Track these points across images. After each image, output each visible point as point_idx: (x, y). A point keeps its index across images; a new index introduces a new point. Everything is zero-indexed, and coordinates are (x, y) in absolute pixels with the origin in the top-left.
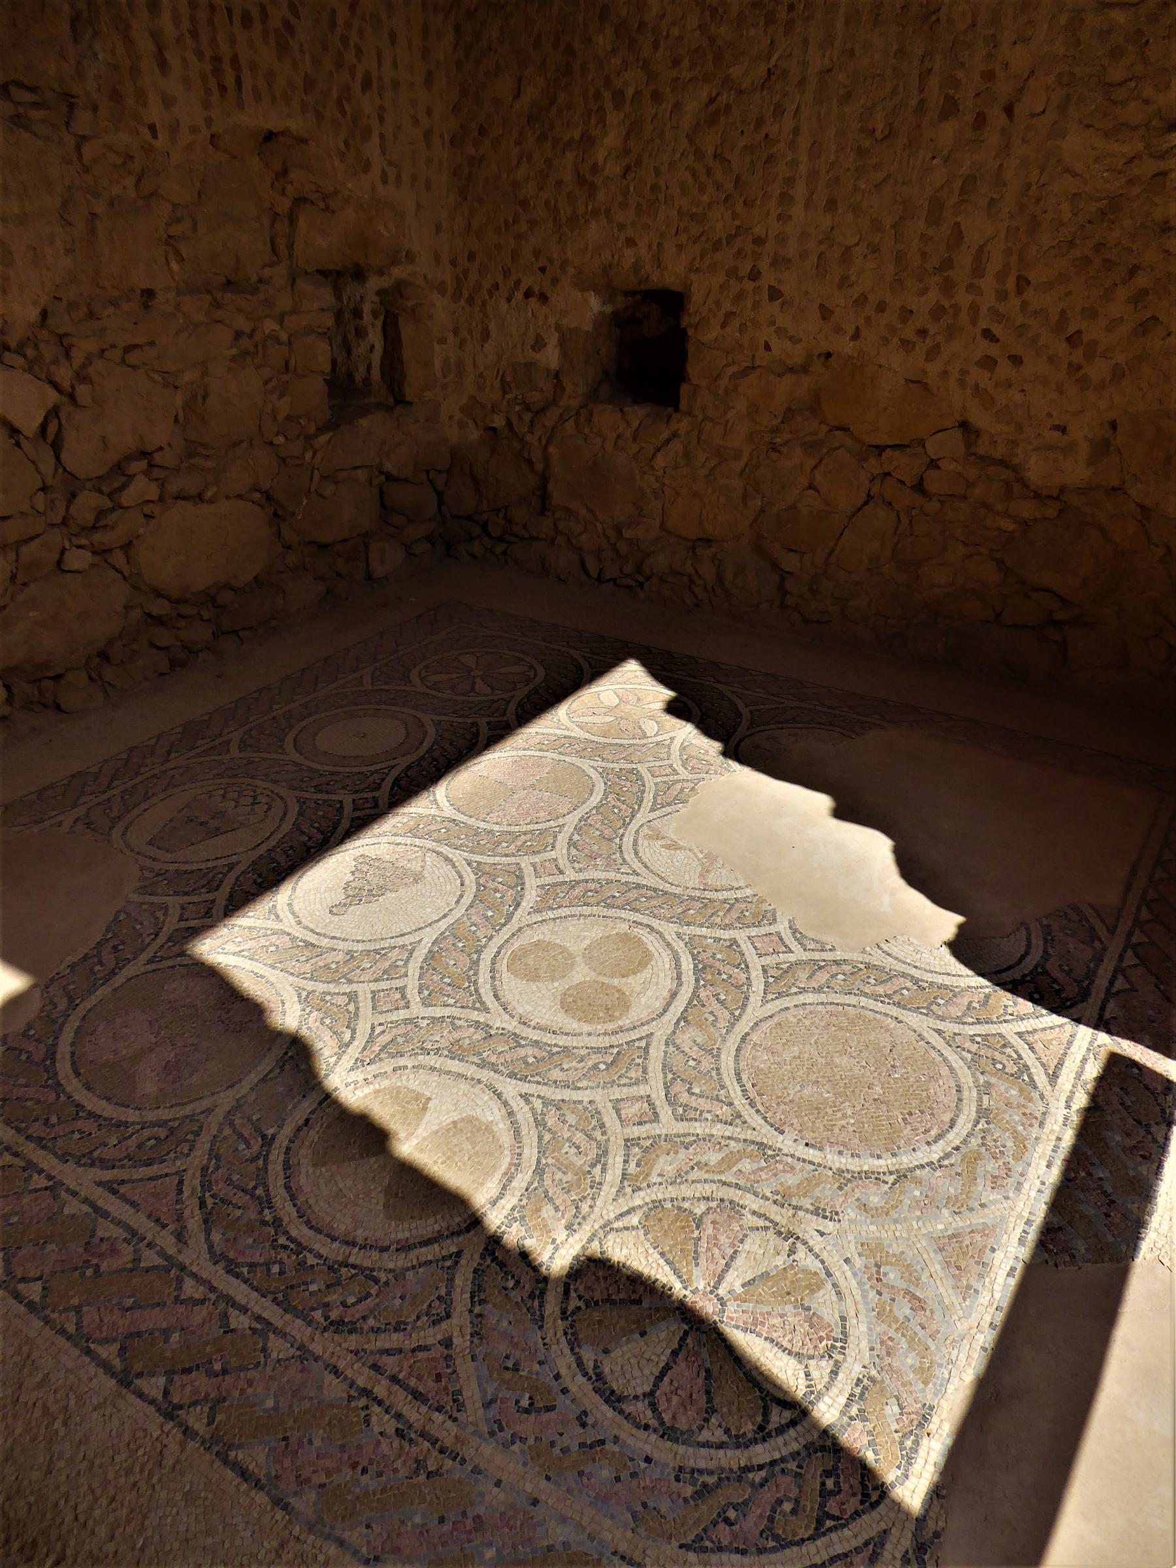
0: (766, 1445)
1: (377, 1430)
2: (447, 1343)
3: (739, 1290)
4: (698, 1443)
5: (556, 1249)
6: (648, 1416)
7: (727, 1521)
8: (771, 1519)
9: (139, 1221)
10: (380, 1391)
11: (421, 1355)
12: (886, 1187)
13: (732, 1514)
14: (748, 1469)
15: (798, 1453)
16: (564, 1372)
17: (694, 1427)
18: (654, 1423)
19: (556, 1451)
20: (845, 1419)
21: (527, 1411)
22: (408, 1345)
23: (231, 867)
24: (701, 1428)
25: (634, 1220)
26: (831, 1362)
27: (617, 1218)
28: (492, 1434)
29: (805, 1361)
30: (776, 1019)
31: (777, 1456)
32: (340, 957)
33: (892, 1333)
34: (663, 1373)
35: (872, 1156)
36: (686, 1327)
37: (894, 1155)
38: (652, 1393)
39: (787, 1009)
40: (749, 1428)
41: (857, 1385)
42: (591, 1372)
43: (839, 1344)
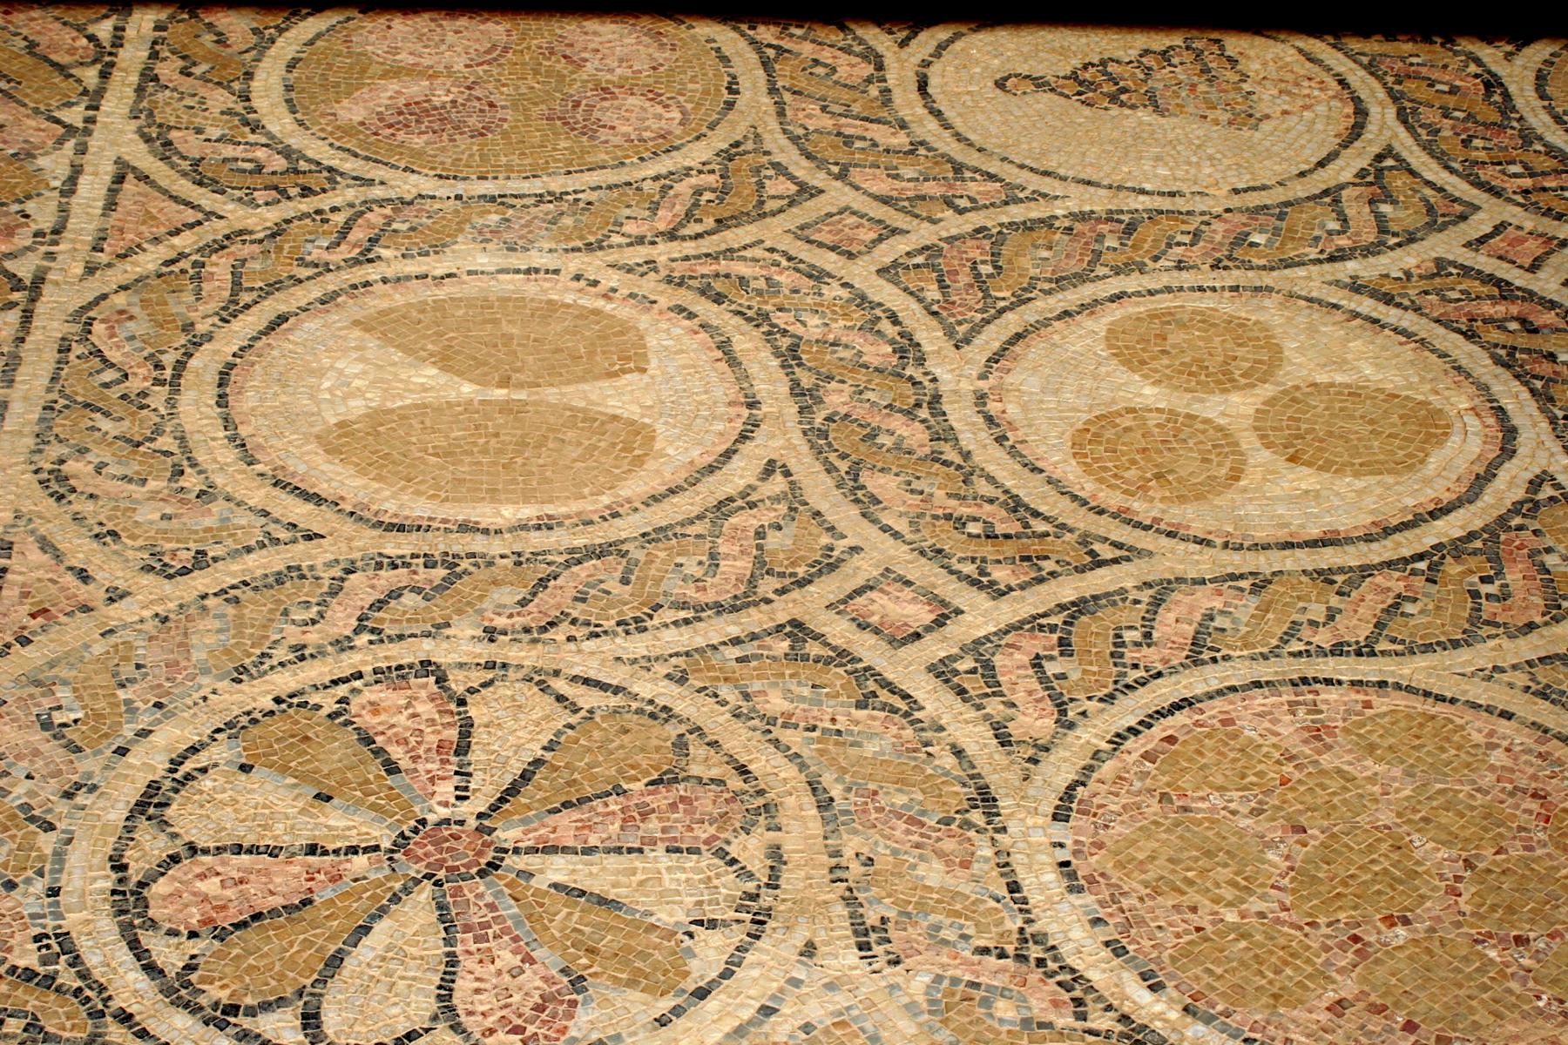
0: (200, 1027)
2: (115, 596)
4: (137, 941)
5: (428, 634)
11: (70, 580)
12: (1065, 1020)
18: (134, 874)
21: (46, 725)
25: (588, 698)
27: (574, 679)
29: (441, 1026)
30: (1440, 708)
32: (901, 140)
38: (193, 849)
40: (218, 993)
42: (188, 766)
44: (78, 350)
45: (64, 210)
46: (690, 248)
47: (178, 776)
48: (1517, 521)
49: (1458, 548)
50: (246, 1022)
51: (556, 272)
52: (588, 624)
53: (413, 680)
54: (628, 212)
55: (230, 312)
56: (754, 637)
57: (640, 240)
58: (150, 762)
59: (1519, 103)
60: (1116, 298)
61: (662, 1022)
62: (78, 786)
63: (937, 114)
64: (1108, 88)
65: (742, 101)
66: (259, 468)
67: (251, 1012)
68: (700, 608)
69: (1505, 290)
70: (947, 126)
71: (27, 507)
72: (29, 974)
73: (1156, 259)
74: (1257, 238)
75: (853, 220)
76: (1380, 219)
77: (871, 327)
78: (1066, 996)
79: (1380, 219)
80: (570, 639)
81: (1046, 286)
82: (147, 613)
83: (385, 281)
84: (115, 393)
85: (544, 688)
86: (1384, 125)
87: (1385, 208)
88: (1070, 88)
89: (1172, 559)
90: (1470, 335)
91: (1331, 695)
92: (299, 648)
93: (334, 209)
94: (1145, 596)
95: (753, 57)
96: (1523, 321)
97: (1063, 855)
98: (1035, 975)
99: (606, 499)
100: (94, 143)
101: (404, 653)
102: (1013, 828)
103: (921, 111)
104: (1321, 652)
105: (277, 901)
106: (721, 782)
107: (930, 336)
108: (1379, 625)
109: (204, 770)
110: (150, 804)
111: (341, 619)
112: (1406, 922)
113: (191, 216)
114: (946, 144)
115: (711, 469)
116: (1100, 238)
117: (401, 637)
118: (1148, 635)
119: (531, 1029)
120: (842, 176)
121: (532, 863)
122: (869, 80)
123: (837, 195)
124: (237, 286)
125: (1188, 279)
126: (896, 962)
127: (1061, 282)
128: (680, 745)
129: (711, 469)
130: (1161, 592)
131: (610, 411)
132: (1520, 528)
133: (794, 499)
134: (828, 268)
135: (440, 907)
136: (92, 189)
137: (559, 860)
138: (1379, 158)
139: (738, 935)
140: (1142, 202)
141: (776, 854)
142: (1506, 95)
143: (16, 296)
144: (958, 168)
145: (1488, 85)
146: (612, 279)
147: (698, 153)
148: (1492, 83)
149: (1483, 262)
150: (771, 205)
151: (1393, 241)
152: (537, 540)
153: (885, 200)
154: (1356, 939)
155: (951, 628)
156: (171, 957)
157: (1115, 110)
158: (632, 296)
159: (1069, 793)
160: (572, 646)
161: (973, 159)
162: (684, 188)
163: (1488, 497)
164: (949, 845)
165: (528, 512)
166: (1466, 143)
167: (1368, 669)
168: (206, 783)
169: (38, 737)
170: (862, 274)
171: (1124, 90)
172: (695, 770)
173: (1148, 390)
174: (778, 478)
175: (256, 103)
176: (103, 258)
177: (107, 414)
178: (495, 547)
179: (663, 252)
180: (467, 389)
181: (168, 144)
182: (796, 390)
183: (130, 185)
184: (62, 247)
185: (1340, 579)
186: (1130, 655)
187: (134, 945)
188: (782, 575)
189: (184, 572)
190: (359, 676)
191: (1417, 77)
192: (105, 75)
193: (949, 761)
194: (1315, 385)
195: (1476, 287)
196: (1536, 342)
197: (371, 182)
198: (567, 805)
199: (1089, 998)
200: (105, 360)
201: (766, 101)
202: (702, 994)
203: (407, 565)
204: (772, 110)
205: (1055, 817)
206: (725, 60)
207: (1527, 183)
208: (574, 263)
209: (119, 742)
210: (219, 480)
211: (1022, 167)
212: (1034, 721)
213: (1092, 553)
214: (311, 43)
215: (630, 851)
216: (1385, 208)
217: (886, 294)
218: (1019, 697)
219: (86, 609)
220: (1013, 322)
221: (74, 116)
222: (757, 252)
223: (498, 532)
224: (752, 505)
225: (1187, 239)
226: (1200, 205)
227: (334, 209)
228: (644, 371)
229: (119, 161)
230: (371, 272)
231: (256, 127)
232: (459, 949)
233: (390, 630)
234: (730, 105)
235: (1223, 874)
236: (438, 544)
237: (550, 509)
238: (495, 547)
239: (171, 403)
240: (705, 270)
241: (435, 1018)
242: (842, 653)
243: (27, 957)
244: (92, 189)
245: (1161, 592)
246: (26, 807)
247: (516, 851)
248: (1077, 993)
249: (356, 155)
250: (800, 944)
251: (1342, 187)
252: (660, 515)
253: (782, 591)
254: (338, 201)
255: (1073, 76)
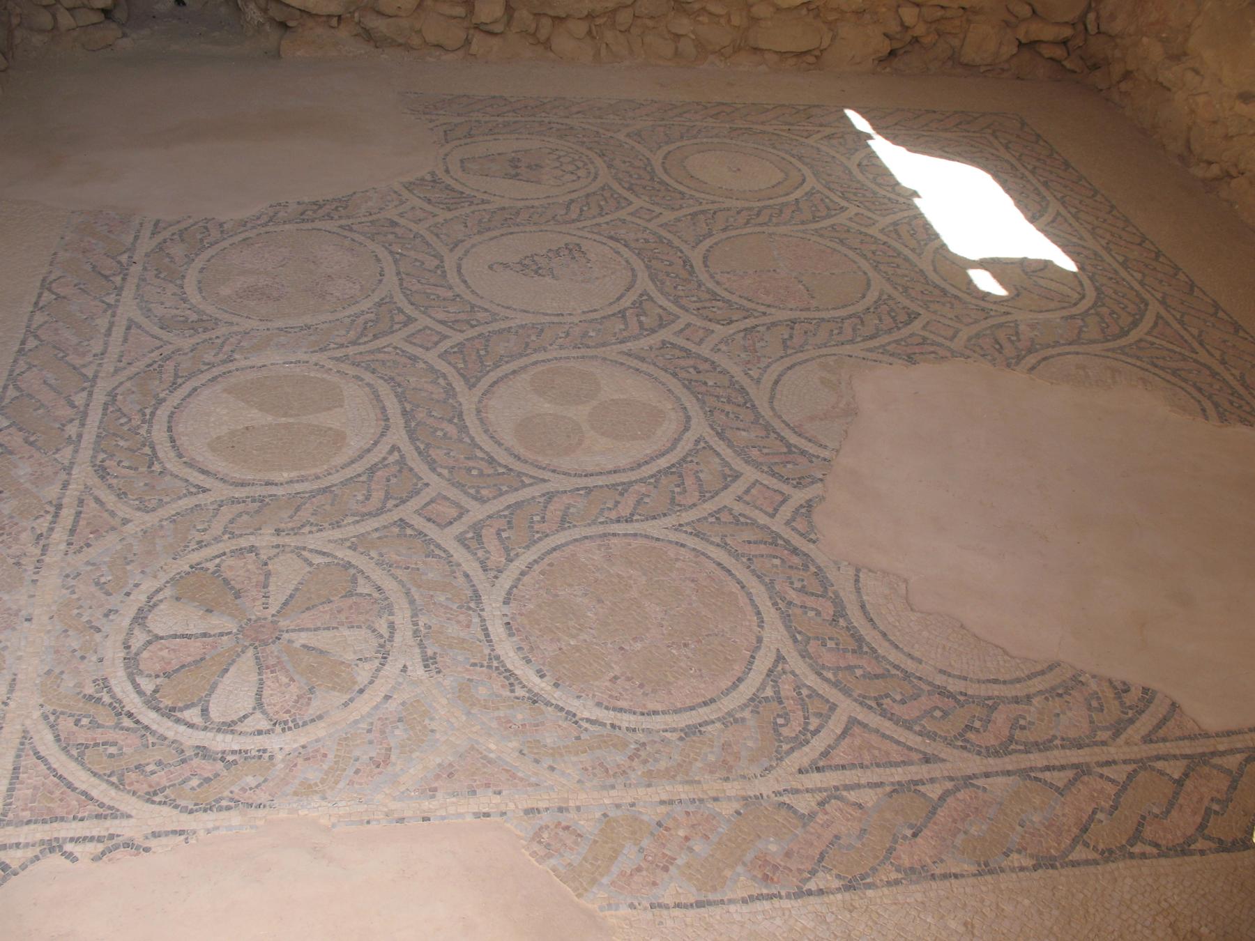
0: (160, 717)
1: (34, 525)
2: (125, 522)
3: (297, 645)
5: (252, 534)
6: (136, 644)
7: (77, 723)
8: (97, 745)
9: (114, 350)
10: (64, 512)
11: (106, 515)
12: (506, 693)
13: (85, 721)
14: (130, 715)
15: (166, 738)
16: (143, 587)
17: (147, 672)
18: (134, 649)
19: (76, 611)
20: (220, 755)
21: (97, 584)
22: (110, 506)
23: (483, 202)
24: (149, 676)
25: (318, 560)
26: (269, 727)
27: (311, 551)
28: (67, 576)
29: (258, 712)
30: (657, 544)
31: (154, 727)
33: (331, 756)
34: (183, 636)
35: (538, 671)
36: (235, 631)
37: (556, 685)
39: (683, 545)
40: (167, 702)
41: (259, 751)
42: (155, 599)
43: (291, 724)
44: (111, 409)
45: (106, 344)
46: (362, 348)
47: (151, 604)
48: (689, 459)
49: (667, 471)
50: (179, 714)
51: (307, 362)
52: (317, 525)
53: (246, 555)
54: (336, 333)
55: (174, 386)
56: (385, 527)
57: (342, 346)
58: (140, 598)
59: (696, 269)
60: (535, 363)
61: (346, 705)
62: (110, 611)
63: (465, 282)
64: (534, 267)
65: (385, 280)
66: (184, 459)
67: (181, 710)
68: (363, 515)
69: (688, 353)
70: (468, 287)
71: (90, 483)
72: (91, 697)
73: (551, 345)
74: (592, 334)
75: (429, 332)
76: (640, 322)
77: (434, 382)
78: (507, 683)
79: (640, 322)
80: (310, 532)
81: (506, 359)
82: (138, 529)
83: (237, 370)
84: (126, 428)
85: (299, 556)
86: (644, 282)
87: (643, 318)
88: (519, 267)
89: (556, 483)
90: (675, 375)
91: (615, 540)
92: (199, 542)
93: (217, 337)
94: (542, 500)
95: (390, 258)
96: (695, 368)
97: (507, 619)
98: (495, 674)
99: (325, 467)
100: (120, 311)
101: (244, 543)
102: (487, 609)
103: (458, 280)
104: (612, 521)
105: (190, 659)
106: (370, 595)
107: (459, 385)
108: (635, 508)
109: (161, 601)
110: (140, 619)
111: (217, 528)
112: (642, 640)
113: (158, 343)
114: (469, 297)
115: (369, 451)
116: (529, 336)
117: (241, 535)
118: (543, 518)
119: (293, 711)
120: (424, 313)
121: (293, 636)
122: (437, 267)
123: (424, 321)
124: (176, 376)
125: (564, 353)
126: (439, 672)
127: (512, 357)
128: (354, 580)
129: (369, 451)
130: (550, 496)
131: (328, 426)
132: (692, 461)
133: (402, 461)
134: (418, 354)
135: (257, 658)
136: (118, 333)
137: (303, 634)
138: (641, 295)
139: (376, 663)
140: (548, 319)
141: (392, 626)
142: (692, 266)
143: (86, 384)
144: (473, 307)
145: (684, 262)
146: (330, 364)
147: (366, 305)
148: (686, 262)
149: (680, 341)
150: (397, 327)
151: (645, 333)
152: (299, 487)
153: (441, 322)
154: (622, 648)
155: (464, 519)
156: (147, 685)
157: (536, 278)
158: (338, 372)
159: (509, 593)
160: (311, 536)
161: (479, 302)
162: (361, 320)
163: (679, 449)
164: (461, 618)
165: (294, 474)
166: (675, 288)
167: (630, 528)
168: (162, 606)
169: (93, 589)
170: (432, 357)
171: (540, 268)
172: (359, 590)
173: (547, 405)
174: (396, 453)
175: (186, 289)
176: (122, 365)
177: (122, 438)
178: (279, 491)
179: (351, 350)
180: (270, 418)
181: (149, 310)
182: (404, 413)
183: (133, 331)
184: (105, 360)
185: (620, 488)
186: (536, 527)
187: (134, 682)
188: (396, 499)
189: (154, 510)
190: (224, 554)
191: (657, 258)
192: (124, 279)
193: (461, 580)
194: (613, 400)
195: (677, 353)
196: (701, 377)
197: (232, 324)
198: (308, 609)
199: (516, 683)
200: (122, 413)
201: (395, 278)
202: (361, 691)
203: (244, 502)
204: (397, 283)
205: (504, 603)
206: (378, 260)
207: (698, 305)
208: (314, 358)
209: (126, 590)
210: (168, 466)
211: (498, 305)
212: (497, 558)
213: (522, 481)
214: (209, 261)
215: (333, 628)
216: (643, 318)
217: (442, 366)
218: (491, 549)
219: (113, 529)
220: (493, 376)
221: (111, 299)
222: (390, 349)
223: (282, 484)
224: (386, 466)
225: (563, 335)
226: (569, 319)
227: (217, 337)
228: (342, 406)
229: (130, 320)
230: (231, 366)
231: (185, 300)
232: (264, 677)
233: (237, 532)
234: (380, 281)
235: (571, 623)
236: (259, 491)
237: (303, 473)
238: (279, 491)
239: (149, 432)
240: (368, 358)
241: (254, 709)
242: (421, 533)
243: (90, 690)
244: (118, 333)
245: (550, 496)
246: (89, 622)
247: (287, 631)
248: (512, 680)
249: (226, 312)
250: (401, 666)
251: (626, 309)
252: (349, 472)
253: (396, 506)
254: (219, 334)
255: (520, 263)
